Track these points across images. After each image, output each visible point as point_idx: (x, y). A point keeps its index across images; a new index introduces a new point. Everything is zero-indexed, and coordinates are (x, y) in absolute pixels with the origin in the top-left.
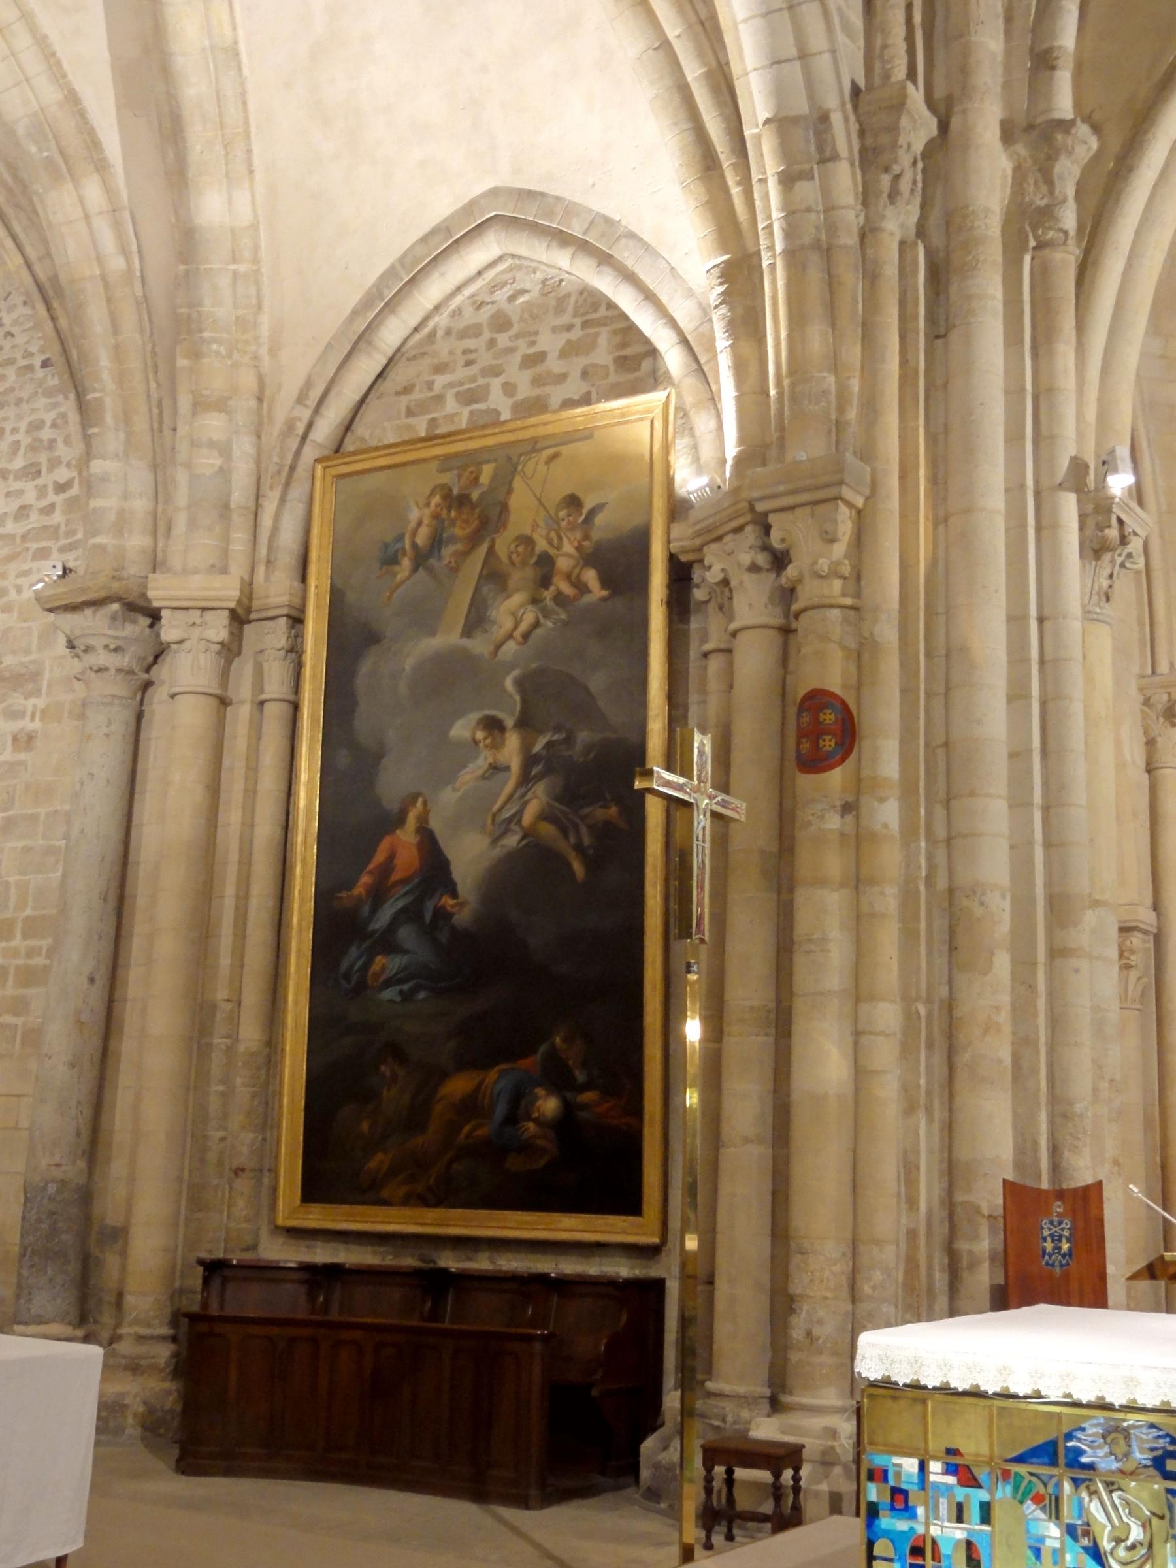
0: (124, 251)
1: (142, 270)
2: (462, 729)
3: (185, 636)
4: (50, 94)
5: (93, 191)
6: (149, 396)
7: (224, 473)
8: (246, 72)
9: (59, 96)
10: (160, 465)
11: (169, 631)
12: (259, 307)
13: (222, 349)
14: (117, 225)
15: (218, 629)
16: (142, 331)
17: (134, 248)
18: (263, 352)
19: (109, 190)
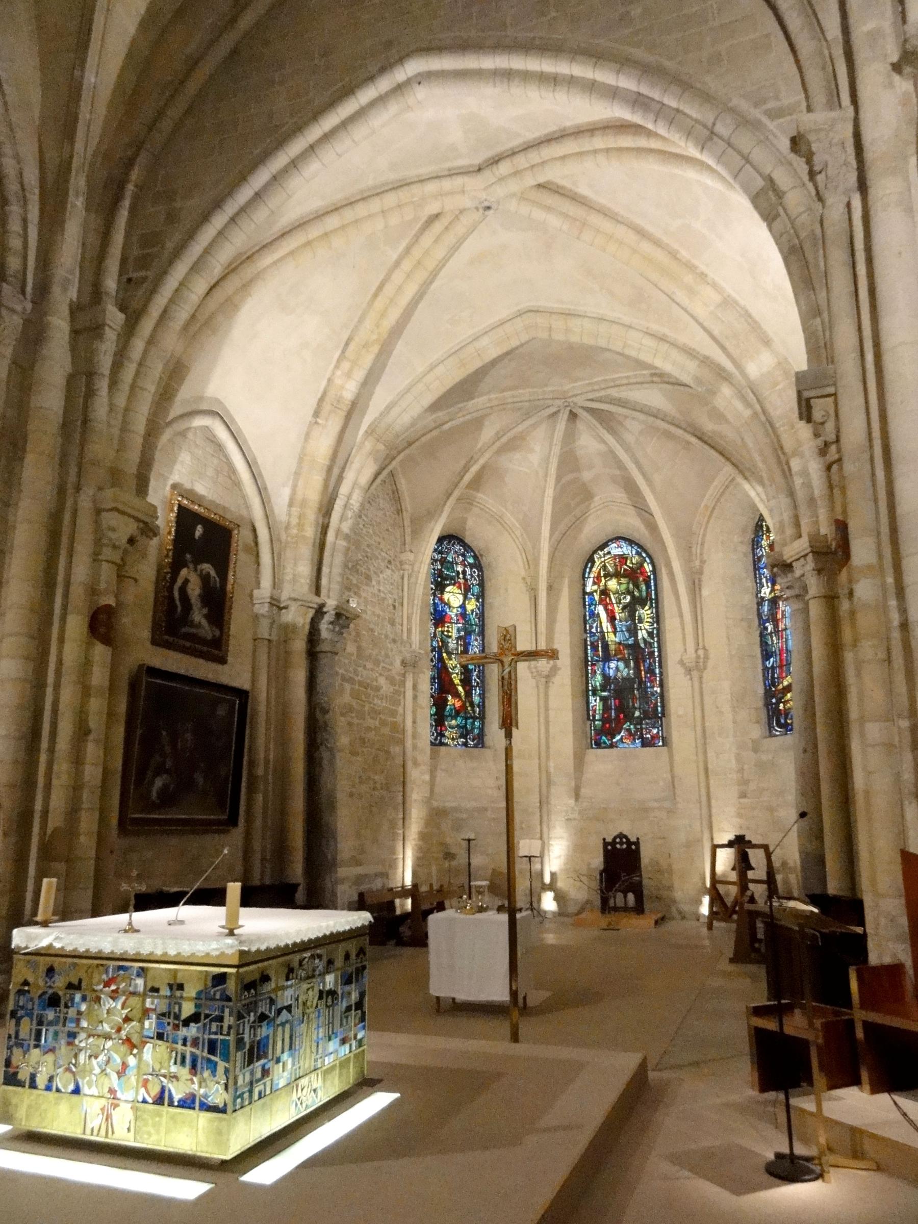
0: (748, 405)
1: (762, 407)
3: (802, 572)
4: (692, 366)
5: (726, 390)
6: (779, 462)
7: (808, 485)
8: (742, 303)
9: (697, 363)
10: (791, 494)
11: (798, 573)
13: (786, 428)
15: (810, 564)
16: (768, 435)
17: (755, 401)
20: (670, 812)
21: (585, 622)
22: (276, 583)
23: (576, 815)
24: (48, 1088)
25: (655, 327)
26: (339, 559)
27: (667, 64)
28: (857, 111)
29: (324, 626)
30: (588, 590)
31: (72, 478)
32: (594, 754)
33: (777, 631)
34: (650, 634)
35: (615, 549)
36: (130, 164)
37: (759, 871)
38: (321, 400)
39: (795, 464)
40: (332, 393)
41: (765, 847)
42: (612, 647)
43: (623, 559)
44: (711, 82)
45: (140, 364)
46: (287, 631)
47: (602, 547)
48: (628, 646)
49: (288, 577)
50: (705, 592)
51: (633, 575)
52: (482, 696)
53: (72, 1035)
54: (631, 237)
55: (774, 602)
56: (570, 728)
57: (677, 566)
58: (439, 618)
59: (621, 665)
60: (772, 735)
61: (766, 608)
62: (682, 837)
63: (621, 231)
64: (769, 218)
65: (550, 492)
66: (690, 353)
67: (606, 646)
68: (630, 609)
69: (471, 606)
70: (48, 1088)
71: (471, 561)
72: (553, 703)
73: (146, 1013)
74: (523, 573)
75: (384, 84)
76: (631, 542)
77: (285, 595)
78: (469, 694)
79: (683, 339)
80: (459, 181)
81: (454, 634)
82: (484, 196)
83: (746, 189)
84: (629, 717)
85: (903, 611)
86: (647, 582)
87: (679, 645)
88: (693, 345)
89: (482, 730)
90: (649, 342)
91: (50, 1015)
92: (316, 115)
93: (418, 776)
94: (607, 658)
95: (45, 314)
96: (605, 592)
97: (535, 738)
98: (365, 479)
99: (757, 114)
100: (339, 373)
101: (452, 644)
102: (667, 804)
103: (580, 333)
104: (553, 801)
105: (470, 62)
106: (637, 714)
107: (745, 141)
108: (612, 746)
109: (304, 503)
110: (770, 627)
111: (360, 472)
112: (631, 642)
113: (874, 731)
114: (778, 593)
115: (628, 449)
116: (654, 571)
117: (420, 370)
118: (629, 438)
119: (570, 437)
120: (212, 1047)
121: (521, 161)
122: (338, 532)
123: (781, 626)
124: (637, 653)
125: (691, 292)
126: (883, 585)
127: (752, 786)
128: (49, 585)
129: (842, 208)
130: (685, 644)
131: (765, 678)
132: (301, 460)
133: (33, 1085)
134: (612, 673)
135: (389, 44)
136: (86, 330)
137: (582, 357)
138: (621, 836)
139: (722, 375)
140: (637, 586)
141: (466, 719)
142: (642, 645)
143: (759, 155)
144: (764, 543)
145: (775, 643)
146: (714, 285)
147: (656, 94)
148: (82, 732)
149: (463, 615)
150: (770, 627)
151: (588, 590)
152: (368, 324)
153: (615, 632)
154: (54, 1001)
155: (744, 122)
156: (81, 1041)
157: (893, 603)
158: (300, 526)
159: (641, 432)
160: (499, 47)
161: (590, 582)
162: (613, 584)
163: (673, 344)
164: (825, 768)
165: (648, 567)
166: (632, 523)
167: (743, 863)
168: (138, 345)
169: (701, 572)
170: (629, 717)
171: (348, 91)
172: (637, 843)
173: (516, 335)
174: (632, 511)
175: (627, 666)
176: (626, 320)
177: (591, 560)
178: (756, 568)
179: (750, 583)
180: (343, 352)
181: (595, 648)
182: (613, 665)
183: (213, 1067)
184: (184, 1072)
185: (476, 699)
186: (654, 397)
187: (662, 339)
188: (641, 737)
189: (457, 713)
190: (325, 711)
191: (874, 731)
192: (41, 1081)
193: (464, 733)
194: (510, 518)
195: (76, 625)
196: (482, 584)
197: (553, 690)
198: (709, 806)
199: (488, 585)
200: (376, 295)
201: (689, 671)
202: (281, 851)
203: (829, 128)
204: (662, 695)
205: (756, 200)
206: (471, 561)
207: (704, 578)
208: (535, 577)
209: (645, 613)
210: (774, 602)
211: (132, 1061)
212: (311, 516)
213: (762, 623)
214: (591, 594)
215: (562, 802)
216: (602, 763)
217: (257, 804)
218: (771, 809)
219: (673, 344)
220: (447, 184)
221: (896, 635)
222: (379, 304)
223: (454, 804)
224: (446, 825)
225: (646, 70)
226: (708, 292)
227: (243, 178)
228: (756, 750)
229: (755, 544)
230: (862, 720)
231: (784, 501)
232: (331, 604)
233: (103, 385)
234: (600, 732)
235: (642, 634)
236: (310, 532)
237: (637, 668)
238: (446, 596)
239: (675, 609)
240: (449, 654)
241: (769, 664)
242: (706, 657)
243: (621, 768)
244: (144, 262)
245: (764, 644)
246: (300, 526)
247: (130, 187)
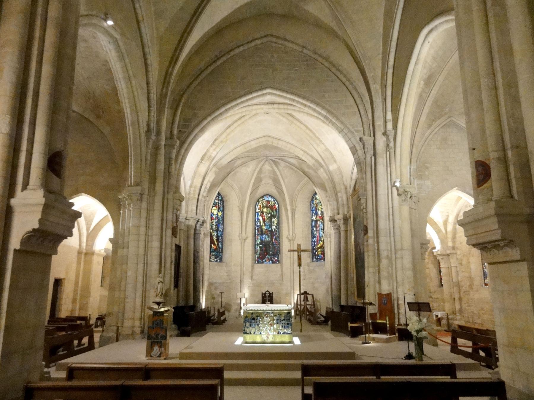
0: (327, 174)
2: (360, 232)
4: (313, 161)
5: (322, 170)
7: (342, 200)
10: (337, 201)
12: (343, 177)
14: (326, 173)
15: (342, 222)
18: (345, 183)
19: (324, 169)
20: (281, 284)
21: (255, 221)
22: (188, 212)
23: (251, 285)
24: (254, 333)
25: (303, 148)
26: (202, 204)
27: (334, 112)
28: (374, 139)
29: (198, 226)
30: (257, 211)
31: (166, 190)
32: (257, 265)
33: (317, 230)
34: (276, 227)
35: (266, 198)
36: (182, 96)
37: (310, 302)
38: (204, 155)
39: (339, 195)
40: (208, 154)
41: (312, 295)
42: (264, 231)
43: (269, 202)
44: (343, 119)
45: (183, 156)
46: (188, 227)
47: (262, 197)
48: (269, 231)
49: (190, 210)
50: (296, 216)
51: (272, 207)
52: (222, 245)
53: (258, 325)
54: (304, 128)
55: (316, 221)
56: (251, 257)
57: (289, 208)
58: (212, 217)
59: (267, 237)
60: (313, 261)
61: (314, 223)
62: (284, 292)
63: (302, 126)
64: (354, 154)
65: (253, 181)
67: (262, 230)
68: (270, 218)
69: (220, 214)
70: (254, 333)
71: (220, 199)
72: (246, 249)
73: (274, 320)
74: (238, 204)
75: (260, 93)
76: (272, 197)
77: (189, 216)
78: (218, 244)
79: (311, 153)
80: (262, 106)
81: (215, 224)
82: (267, 110)
83: (349, 145)
84: (268, 254)
85: (378, 246)
86: (276, 210)
87: (287, 233)
88: (314, 156)
89: (222, 256)
90: (302, 152)
91: (253, 321)
92: (240, 97)
93: (207, 272)
94: (262, 234)
95: (160, 141)
96: (262, 212)
97: (240, 260)
98: (211, 180)
99: (353, 130)
100: (211, 149)
101: (214, 227)
102: (280, 282)
103: (281, 144)
104: (245, 281)
105: (284, 94)
107: (350, 135)
108: (262, 263)
109: (195, 187)
110: (315, 229)
111: (210, 178)
113: (371, 270)
114: (318, 219)
115: (280, 171)
116: (279, 207)
117: (232, 148)
118: (280, 168)
119: (263, 165)
120: (288, 324)
121: (281, 106)
122: (203, 195)
123: (318, 229)
124: (271, 233)
125: (318, 145)
126: (374, 241)
127: (307, 276)
128: (162, 220)
129: (369, 158)
130: (289, 232)
131: (312, 244)
132: (195, 173)
133: (250, 333)
134: (263, 239)
135: (261, 83)
136: (169, 146)
137: (276, 148)
138: (267, 291)
139: (321, 166)
140: (273, 211)
141: (217, 252)
143: (352, 139)
144: (314, 203)
145: (316, 234)
146: (323, 144)
147: (331, 118)
148: (171, 262)
149: (217, 217)
150: (315, 229)
151: (257, 211)
152: (224, 136)
153: (265, 226)
154: (254, 319)
155: (350, 131)
156: (261, 325)
157: (376, 244)
158: (194, 194)
159: (284, 167)
160: (292, 93)
161: (258, 208)
162: (265, 210)
163: (308, 154)
164: (342, 274)
165: (277, 205)
166: (273, 191)
167: (306, 299)
168: (183, 151)
169: (295, 210)
171: (251, 93)
172: (272, 294)
173: (263, 142)
174: (274, 187)
175: (268, 237)
176: (296, 144)
178: (311, 210)
179: (309, 214)
180: (214, 142)
181: (258, 230)
182: (264, 236)
183: (288, 327)
184: (283, 328)
185: (220, 246)
186: (293, 161)
187: (305, 152)
188: (272, 260)
189: (214, 250)
190: (198, 252)
191: (371, 270)
192: (252, 333)
193: (217, 257)
194: (235, 186)
195: (169, 232)
196: (223, 207)
197: (246, 244)
198: (294, 283)
199: (225, 207)
200: (227, 128)
201: (290, 240)
202: (187, 296)
203: (368, 140)
204: (279, 247)
205: (351, 148)
206: (220, 199)
207: (296, 212)
208: (243, 206)
209: (275, 220)
210: (316, 221)
211: (272, 328)
212: (198, 191)
213: (312, 227)
214: (258, 213)
215: (247, 282)
216: (260, 268)
217: (182, 281)
218: (313, 284)
219: (308, 154)
220: (259, 107)
221: (376, 251)
222: (228, 131)
223: (215, 281)
224: (213, 288)
225: (329, 112)
226: (322, 146)
227: (218, 109)
228: (308, 266)
229: (311, 203)
230: (368, 267)
231: (335, 203)
232: (202, 219)
233: (173, 162)
234: (258, 258)
235: (274, 227)
236: (197, 196)
237: (272, 239)
238: (213, 211)
239: (286, 221)
240: (213, 230)
241: (314, 240)
242: (295, 237)
243: (266, 269)
244: (185, 126)
245: (312, 233)
246: (194, 194)
247: (182, 103)
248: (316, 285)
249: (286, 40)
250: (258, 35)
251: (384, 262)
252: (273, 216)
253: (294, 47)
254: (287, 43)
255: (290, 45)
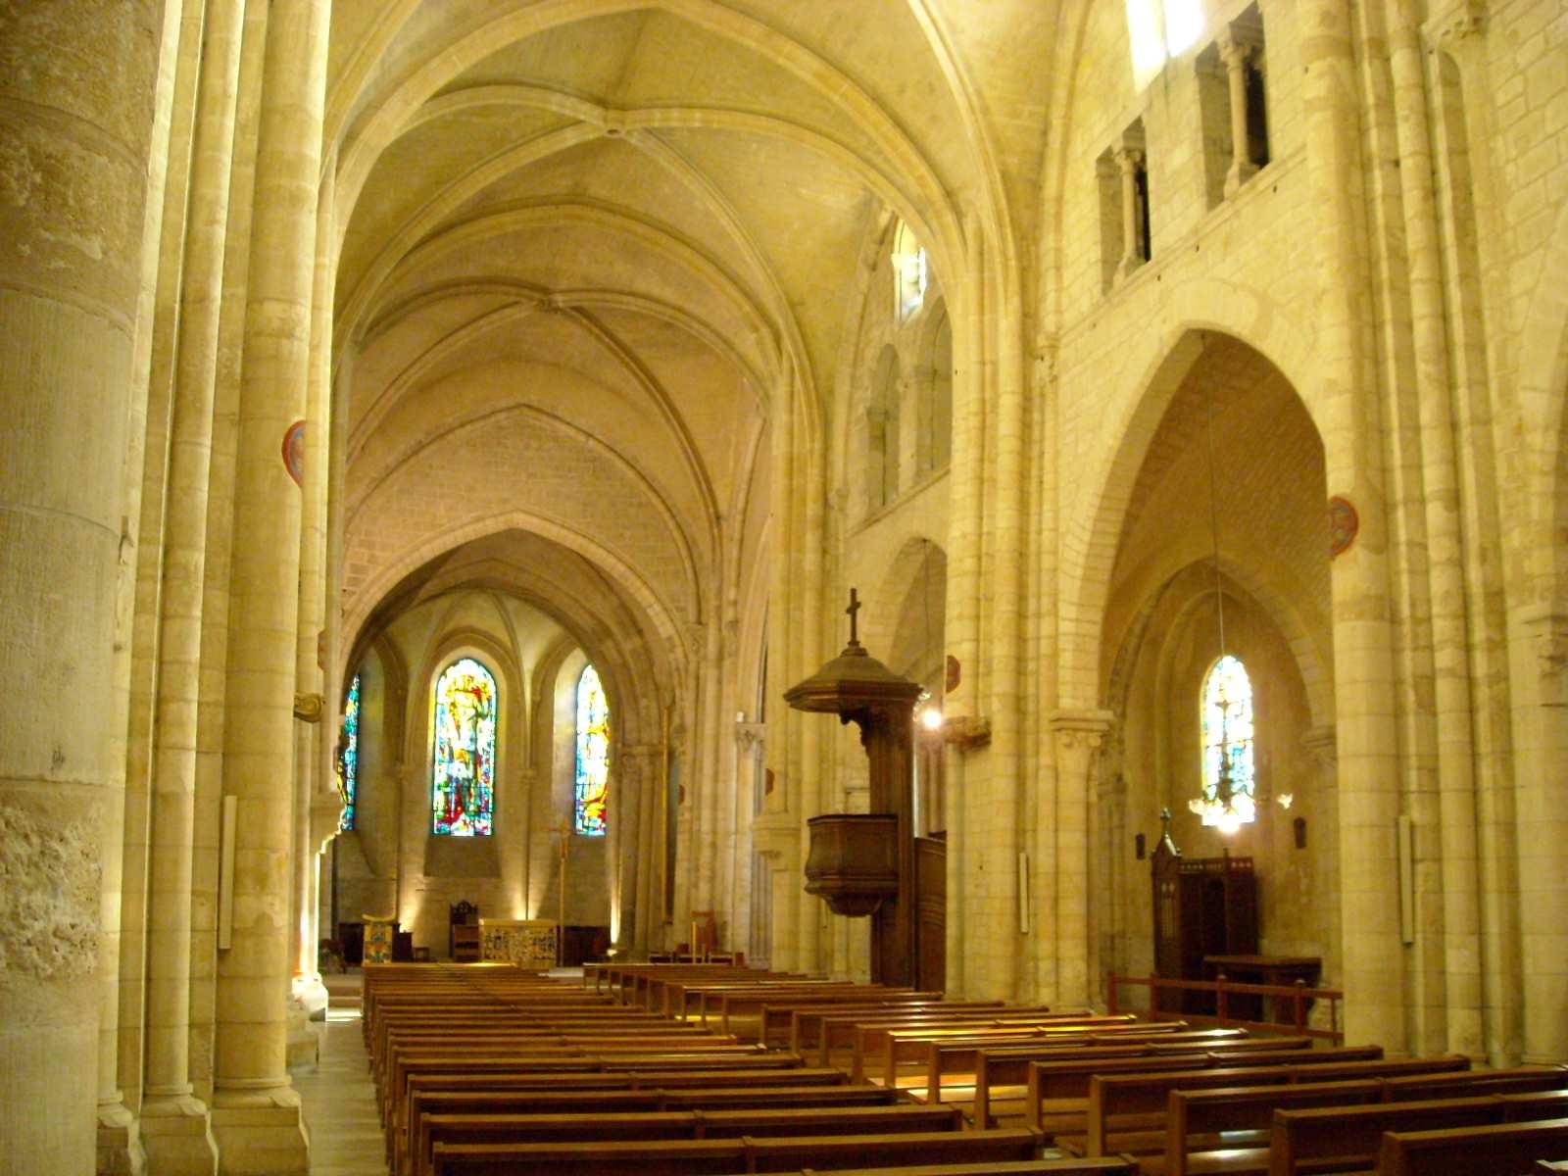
23: (423, 887)
34: (489, 745)
42: (456, 754)
47: (455, 664)
59: (463, 766)
66: (592, 615)
79: (588, 605)
84: (464, 809)
86: (489, 700)
106: (472, 808)
112: (472, 748)
140: (480, 700)
142: (481, 752)
170: (464, 809)
177: (444, 673)
187: (576, 601)
219: (584, 608)
235: (482, 744)
248: (579, 890)
249: (555, 417)
250: (503, 404)
251: (706, 854)
252: (479, 715)
253: (572, 432)
254: (557, 424)
255: (563, 428)
